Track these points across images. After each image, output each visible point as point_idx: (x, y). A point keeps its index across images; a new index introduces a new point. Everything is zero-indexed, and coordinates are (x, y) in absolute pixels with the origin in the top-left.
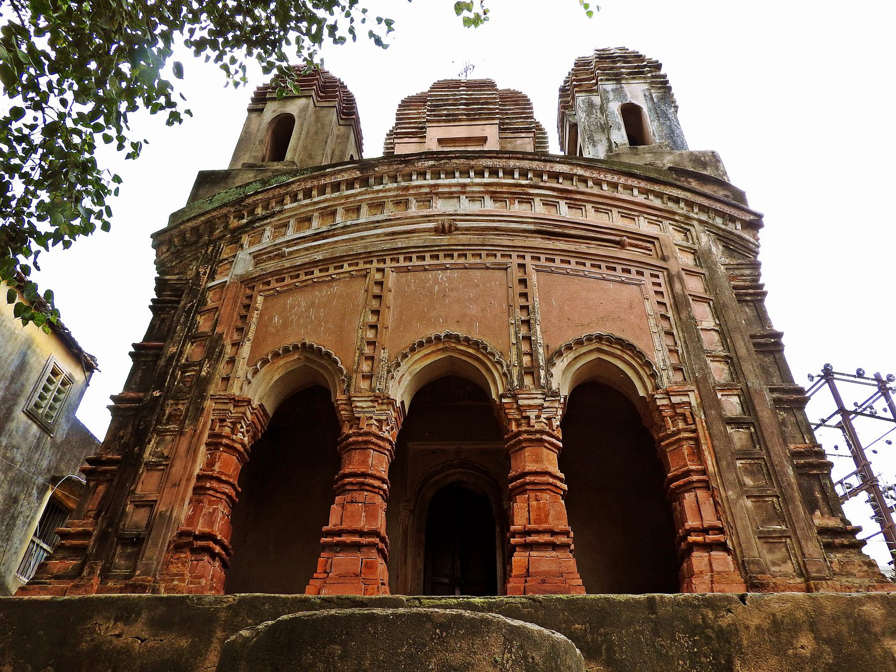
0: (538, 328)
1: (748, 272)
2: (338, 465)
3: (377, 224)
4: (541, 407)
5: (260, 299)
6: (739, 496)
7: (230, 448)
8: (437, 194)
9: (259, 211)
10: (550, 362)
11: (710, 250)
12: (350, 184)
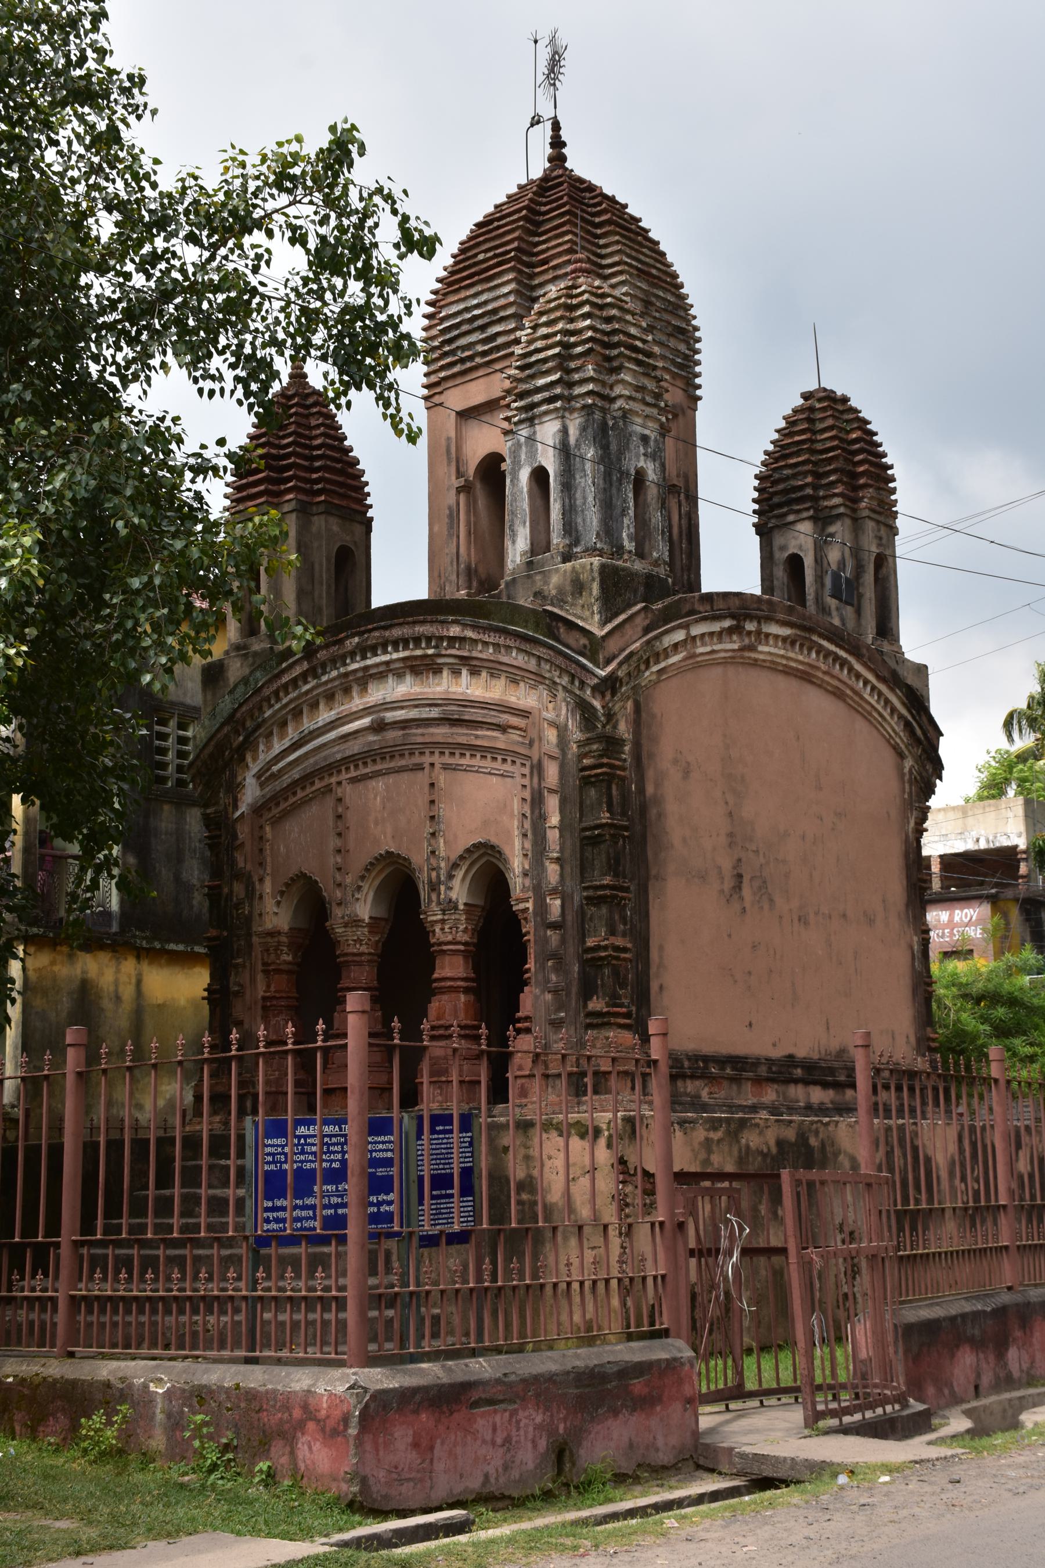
0: (442, 841)
1: (595, 747)
2: (339, 978)
3: (332, 725)
4: (443, 921)
5: (268, 829)
6: (543, 992)
7: (278, 971)
8: (371, 676)
9: (249, 724)
10: (451, 877)
11: (566, 725)
12: (304, 677)
